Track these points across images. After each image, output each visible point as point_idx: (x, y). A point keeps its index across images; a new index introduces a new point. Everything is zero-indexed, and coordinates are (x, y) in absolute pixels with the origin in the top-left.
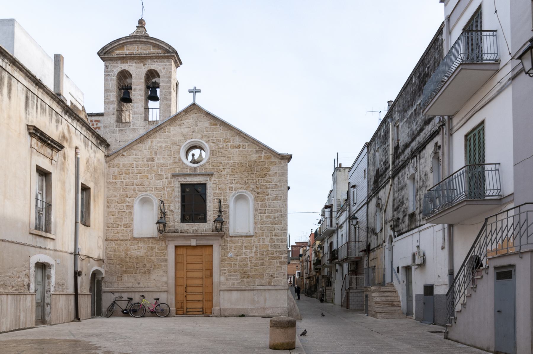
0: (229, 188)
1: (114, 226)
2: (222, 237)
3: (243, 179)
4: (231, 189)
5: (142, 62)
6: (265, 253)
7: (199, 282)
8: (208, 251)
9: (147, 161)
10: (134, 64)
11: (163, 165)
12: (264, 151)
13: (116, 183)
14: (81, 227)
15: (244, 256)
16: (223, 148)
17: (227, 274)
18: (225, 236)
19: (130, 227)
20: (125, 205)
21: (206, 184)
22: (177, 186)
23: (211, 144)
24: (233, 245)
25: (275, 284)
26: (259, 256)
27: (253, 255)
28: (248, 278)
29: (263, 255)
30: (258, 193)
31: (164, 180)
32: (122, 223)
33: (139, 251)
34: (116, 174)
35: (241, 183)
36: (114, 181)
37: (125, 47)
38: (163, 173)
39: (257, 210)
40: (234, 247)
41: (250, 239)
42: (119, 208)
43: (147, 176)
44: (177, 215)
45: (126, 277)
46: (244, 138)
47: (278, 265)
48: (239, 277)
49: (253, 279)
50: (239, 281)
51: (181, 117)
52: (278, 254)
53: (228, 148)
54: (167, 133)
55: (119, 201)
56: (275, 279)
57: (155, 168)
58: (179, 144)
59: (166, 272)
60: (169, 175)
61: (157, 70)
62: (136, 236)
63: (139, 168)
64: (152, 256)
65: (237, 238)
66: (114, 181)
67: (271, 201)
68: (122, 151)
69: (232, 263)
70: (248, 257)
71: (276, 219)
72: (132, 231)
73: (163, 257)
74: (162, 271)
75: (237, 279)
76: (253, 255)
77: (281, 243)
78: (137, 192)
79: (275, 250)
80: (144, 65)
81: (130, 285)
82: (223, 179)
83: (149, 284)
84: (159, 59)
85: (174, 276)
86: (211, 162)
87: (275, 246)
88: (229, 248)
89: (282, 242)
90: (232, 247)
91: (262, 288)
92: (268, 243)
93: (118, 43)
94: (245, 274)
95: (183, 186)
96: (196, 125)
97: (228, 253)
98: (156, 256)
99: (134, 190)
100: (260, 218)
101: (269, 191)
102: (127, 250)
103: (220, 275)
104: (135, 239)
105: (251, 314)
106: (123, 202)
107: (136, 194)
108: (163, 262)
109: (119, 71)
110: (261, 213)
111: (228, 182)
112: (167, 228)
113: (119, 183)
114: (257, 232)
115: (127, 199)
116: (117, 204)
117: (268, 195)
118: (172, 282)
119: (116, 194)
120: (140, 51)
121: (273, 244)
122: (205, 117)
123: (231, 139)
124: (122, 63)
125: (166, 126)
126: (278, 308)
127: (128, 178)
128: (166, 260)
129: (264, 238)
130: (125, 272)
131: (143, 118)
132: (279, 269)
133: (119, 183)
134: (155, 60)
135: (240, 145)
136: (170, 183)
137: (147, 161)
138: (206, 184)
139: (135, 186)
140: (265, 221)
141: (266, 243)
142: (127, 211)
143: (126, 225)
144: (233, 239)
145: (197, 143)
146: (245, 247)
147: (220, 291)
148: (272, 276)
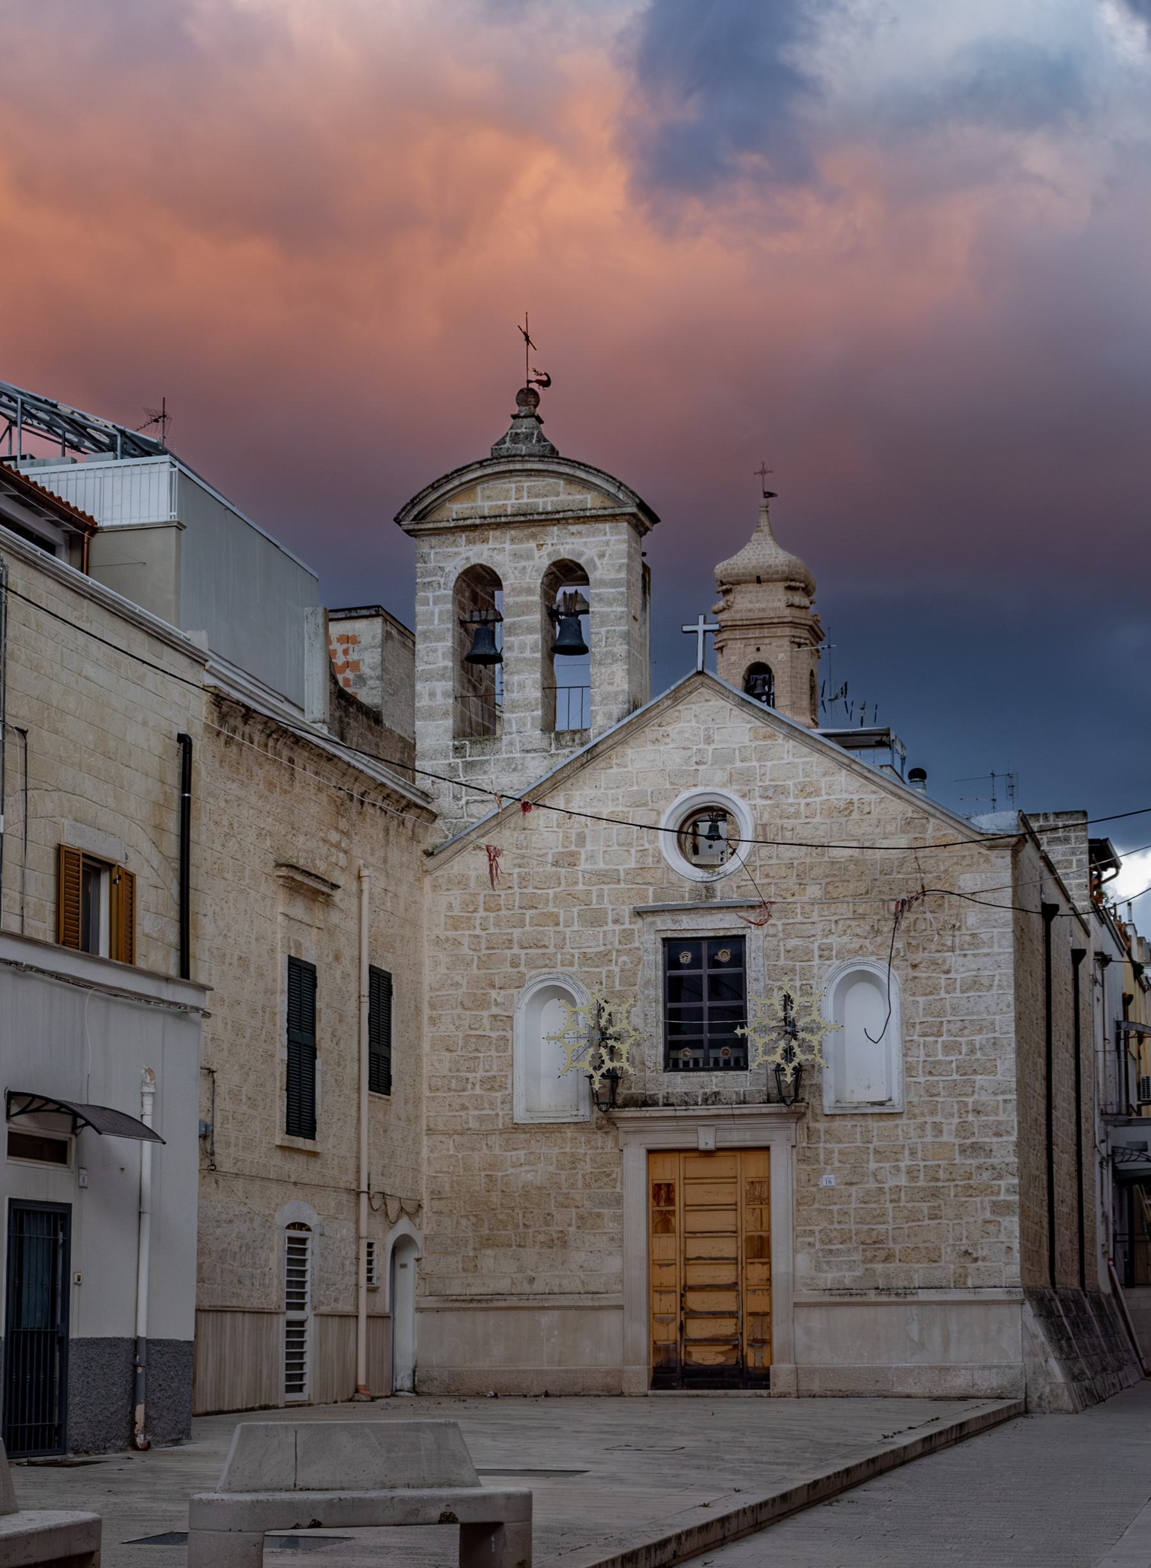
0: (820, 949)
1: (453, 1086)
2: (800, 1116)
3: (863, 917)
4: (825, 953)
5: (534, 536)
6: (942, 1174)
7: (726, 1275)
8: (751, 1167)
9: (556, 864)
10: (508, 546)
11: (604, 877)
12: (932, 820)
13: (457, 943)
14: (209, 1121)
15: (872, 1185)
16: (797, 815)
17: (818, 1246)
18: (809, 1115)
19: (502, 1087)
20: (485, 1014)
21: (744, 936)
22: (650, 946)
23: (759, 802)
24: (837, 1147)
25: (978, 1283)
26: (921, 1183)
27: (903, 1180)
28: (887, 1259)
29: (937, 1180)
30: (914, 966)
31: (610, 927)
32: (480, 1074)
33: (528, 1168)
34: (457, 912)
35: (858, 931)
36: (451, 934)
37: (479, 488)
38: (606, 904)
39: (913, 1025)
40: (841, 1153)
41: (891, 1123)
42: (466, 1023)
43: (557, 916)
44: (653, 1047)
45: (488, 1259)
46: (866, 778)
47: (988, 1215)
48: (857, 1257)
49: (905, 1266)
51: (660, 714)
52: (986, 1175)
53: (814, 816)
54: (615, 770)
55: (467, 1003)
56: (980, 1263)
57: (581, 887)
58: (656, 806)
59: (618, 1240)
60: (626, 910)
61: (581, 561)
62: (520, 1115)
63: (530, 890)
64: (573, 1186)
65: (849, 1123)
66: (451, 934)
67: (958, 994)
68: (474, 835)
69: (835, 1208)
70: (886, 1186)
71: (978, 1055)
72: (508, 1101)
73: (609, 1190)
74: (605, 1238)
75: (851, 1266)
76: (903, 1180)
77: (995, 1140)
78: (522, 969)
79: (974, 1162)
80: (540, 546)
81: (503, 1285)
82: (800, 918)
83: (565, 1282)
84: (584, 523)
85: (644, 1254)
86: (758, 863)
87: (976, 1148)
88: (822, 1157)
89: (998, 1134)
90: (831, 1152)
91: (934, 1296)
92: (952, 1139)
93: (456, 483)
94: (876, 1247)
95: (672, 946)
96: (709, 740)
97: (820, 1173)
98: (587, 1186)
99: (515, 964)
100: (922, 1052)
101: (952, 959)
102: (492, 1166)
103: (795, 1251)
104: (517, 1127)
105: (899, 1389)
106: (482, 1003)
107: (522, 975)
108: (609, 1206)
109: (460, 570)
110: (924, 1035)
111: (818, 929)
112: (622, 1091)
113: (466, 941)
114: (915, 1100)
115: (494, 993)
116: (460, 1010)
117: (948, 972)
118: (637, 1274)
119: (458, 978)
120: (525, 500)
121: (968, 1141)
122: (736, 711)
123: (824, 782)
124: (469, 542)
125: (612, 747)
126: (990, 1368)
127: (496, 925)
128: (619, 1200)
129: (938, 1119)
130: (487, 1242)
131: (539, 723)
132: (991, 1228)
133: (466, 941)
134: (573, 528)
135: (851, 803)
136: (627, 936)
137: (556, 864)
138: (744, 936)
139: (516, 950)
140: (939, 1062)
141: (945, 1138)
142: (494, 1034)
143: (491, 1083)
144: (837, 1124)
145: (717, 799)
146: (876, 1151)
147: (796, 1305)
148: (966, 1253)
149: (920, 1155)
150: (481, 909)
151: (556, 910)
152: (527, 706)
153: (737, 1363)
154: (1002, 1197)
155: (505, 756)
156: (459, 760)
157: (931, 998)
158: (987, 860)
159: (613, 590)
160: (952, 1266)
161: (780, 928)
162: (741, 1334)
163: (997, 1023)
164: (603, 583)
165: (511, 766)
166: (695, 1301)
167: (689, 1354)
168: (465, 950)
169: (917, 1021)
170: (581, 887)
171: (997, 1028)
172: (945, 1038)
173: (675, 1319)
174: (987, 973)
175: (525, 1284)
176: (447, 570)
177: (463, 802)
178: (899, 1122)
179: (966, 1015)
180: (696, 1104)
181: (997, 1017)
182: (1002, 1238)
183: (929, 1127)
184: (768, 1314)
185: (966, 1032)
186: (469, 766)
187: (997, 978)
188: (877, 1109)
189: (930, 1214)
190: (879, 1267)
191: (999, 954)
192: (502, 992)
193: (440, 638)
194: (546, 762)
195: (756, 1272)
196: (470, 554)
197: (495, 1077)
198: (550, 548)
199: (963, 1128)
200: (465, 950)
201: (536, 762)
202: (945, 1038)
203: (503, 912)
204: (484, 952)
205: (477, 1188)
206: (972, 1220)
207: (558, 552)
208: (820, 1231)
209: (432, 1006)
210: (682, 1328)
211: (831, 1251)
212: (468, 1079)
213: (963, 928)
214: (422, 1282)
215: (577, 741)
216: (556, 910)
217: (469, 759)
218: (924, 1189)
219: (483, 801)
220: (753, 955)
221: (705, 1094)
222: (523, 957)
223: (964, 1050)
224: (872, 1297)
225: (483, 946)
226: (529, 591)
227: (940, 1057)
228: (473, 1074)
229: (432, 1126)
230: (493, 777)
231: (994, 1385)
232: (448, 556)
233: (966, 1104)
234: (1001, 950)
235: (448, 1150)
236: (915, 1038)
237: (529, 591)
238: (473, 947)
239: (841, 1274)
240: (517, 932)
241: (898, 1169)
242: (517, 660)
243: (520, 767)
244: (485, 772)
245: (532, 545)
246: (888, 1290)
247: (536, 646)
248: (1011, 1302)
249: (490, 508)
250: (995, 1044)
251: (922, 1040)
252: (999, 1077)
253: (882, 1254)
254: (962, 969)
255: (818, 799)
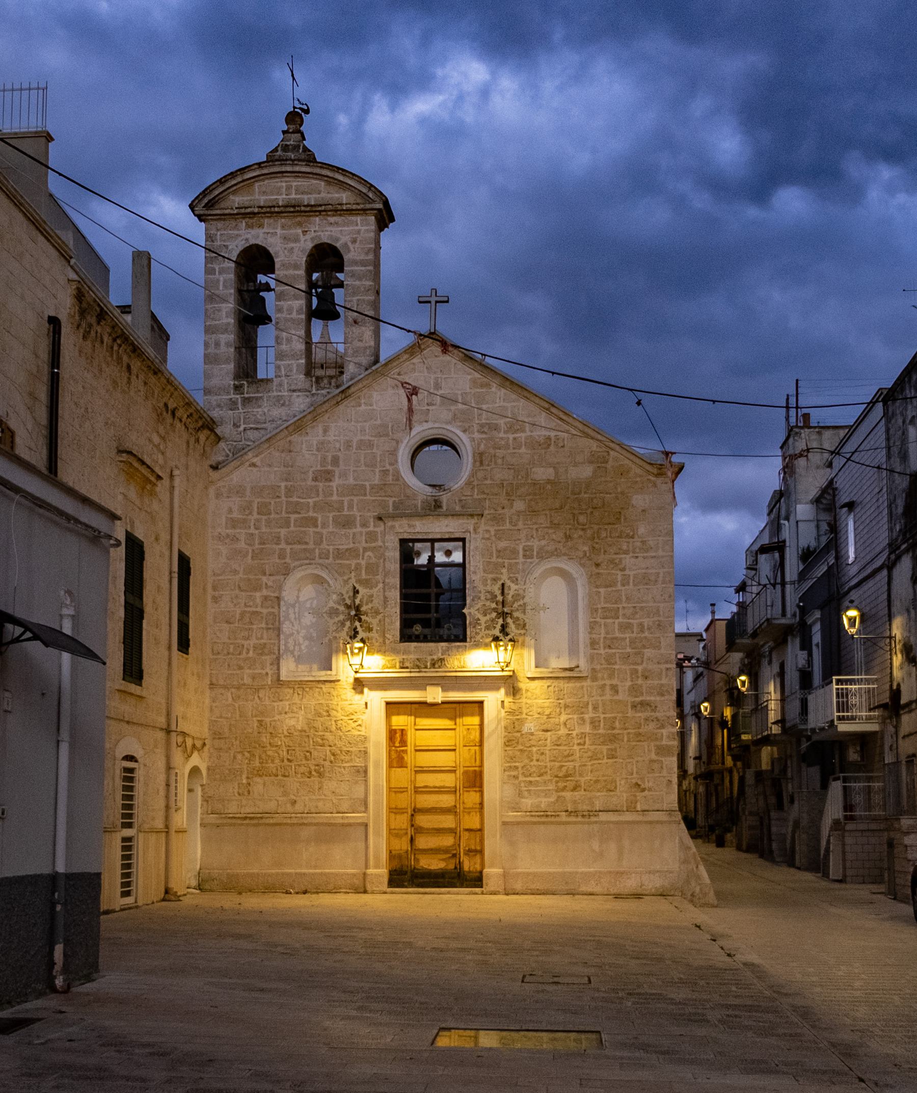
0: (525, 550)
5: (300, 224)
7: (447, 800)
10: (279, 231)
17: (521, 778)
20: (258, 594)
27: (587, 729)
28: (574, 789)
29: (614, 728)
30: (597, 565)
32: (253, 641)
34: (235, 515)
37: (257, 184)
38: (355, 512)
39: (596, 610)
43: (316, 519)
45: (258, 786)
47: (654, 756)
48: (551, 787)
50: (552, 800)
52: (652, 726)
53: (520, 447)
54: (363, 407)
57: (335, 498)
60: (370, 515)
61: (338, 245)
63: (295, 499)
69: (534, 749)
71: (646, 634)
77: (658, 698)
78: (288, 560)
80: (305, 232)
81: (271, 806)
83: (320, 804)
84: (340, 215)
86: (475, 483)
93: (239, 179)
99: (282, 556)
100: (603, 631)
101: (628, 560)
105: (584, 889)
109: (241, 248)
114: (598, 667)
115: (264, 579)
116: (237, 592)
117: (623, 570)
120: (293, 196)
122: (460, 365)
124: (248, 226)
125: (360, 390)
129: (614, 682)
132: (656, 766)
133: (243, 537)
134: (332, 219)
137: (315, 479)
139: (283, 545)
140: (616, 638)
141: (620, 697)
149: (600, 710)
150: (255, 513)
151: (315, 515)
152: (294, 356)
153: (456, 868)
154: (664, 743)
155: (275, 394)
156: (238, 396)
157: (609, 589)
158: (655, 485)
159: (363, 268)
160: (625, 795)
161: (493, 533)
162: (459, 845)
163: (661, 609)
164: (355, 263)
165: (280, 402)
166: (423, 820)
167: (417, 860)
168: (242, 545)
169: (599, 606)
170: (335, 498)
171: (661, 613)
172: (621, 620)
173: (407, 833)
174: (654, 571)
175: (289, 805)
176: (230, 247)
177: (242, 428)
178: (585, 684)
179: (637, 602)
180: (426, 667)
181: (662, 605)
182: (664, 773)
183: (608, 688)
184: (481, 830)
185: (637, 616)
186: (247, 401)
187: (661, 575)
188: (568, 674)
189: (608, 755)
190: (568, 795)
191: (663, 557)
192: (272, 578)
193: (225, 301)
194: (308, 400)
195: (471, 798)
196: (249, 236)
197: (265, 644)
198: (313, 234)
199: (634, 690)
200: (242, 545)
201: (300, 400)
202: (621, 620)
203: (272, 516)
204: (257, 546)
205: (250, 731)
206: (639, 759)
207: (319, 237)
208: (523, 767)
209: (215, 588)
210: (412, 840)
211: (531, 782)
212: (243, 646)
213: (636, 536)
214: (205, 803)
215: (333, 384)
216: (315, 515)
217: (246, 396)
218: (604, 735)
219: (257, 429)
220: (472, 553)
221: (433, 660)
222: (288, 551)
223: (635, 630)
224: (564, 817)
225: (257, 542)
226: (296, 267)
227: (617, 635)
228: (248, 642)
229: (214, 681)
230: (266, 410)
231: (658, 885)
232: (231, 238)
233: (636, 671)
234: (664, 554)
235: (227, 700)
236: (598, 619)
237: (296, 267)
238: (248, 542)
239: (539, 799)
240: (283, 532)
241: (583, 719)
242: (286, 320)
243: (287, 403)
244: (260, 407)
245: (300, 231)
246: (575, 813)
247: (301, 309)
248: (670, 822)
249: (266, 201)
250: (659, 625)
251: (603, 621)
252: (663, 651)
253: (570, 785)
254: (634, 568)
255: (523, 435)
